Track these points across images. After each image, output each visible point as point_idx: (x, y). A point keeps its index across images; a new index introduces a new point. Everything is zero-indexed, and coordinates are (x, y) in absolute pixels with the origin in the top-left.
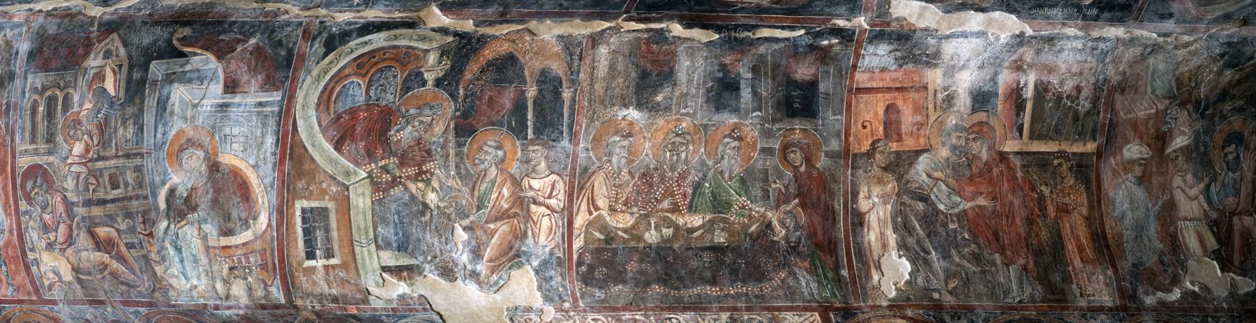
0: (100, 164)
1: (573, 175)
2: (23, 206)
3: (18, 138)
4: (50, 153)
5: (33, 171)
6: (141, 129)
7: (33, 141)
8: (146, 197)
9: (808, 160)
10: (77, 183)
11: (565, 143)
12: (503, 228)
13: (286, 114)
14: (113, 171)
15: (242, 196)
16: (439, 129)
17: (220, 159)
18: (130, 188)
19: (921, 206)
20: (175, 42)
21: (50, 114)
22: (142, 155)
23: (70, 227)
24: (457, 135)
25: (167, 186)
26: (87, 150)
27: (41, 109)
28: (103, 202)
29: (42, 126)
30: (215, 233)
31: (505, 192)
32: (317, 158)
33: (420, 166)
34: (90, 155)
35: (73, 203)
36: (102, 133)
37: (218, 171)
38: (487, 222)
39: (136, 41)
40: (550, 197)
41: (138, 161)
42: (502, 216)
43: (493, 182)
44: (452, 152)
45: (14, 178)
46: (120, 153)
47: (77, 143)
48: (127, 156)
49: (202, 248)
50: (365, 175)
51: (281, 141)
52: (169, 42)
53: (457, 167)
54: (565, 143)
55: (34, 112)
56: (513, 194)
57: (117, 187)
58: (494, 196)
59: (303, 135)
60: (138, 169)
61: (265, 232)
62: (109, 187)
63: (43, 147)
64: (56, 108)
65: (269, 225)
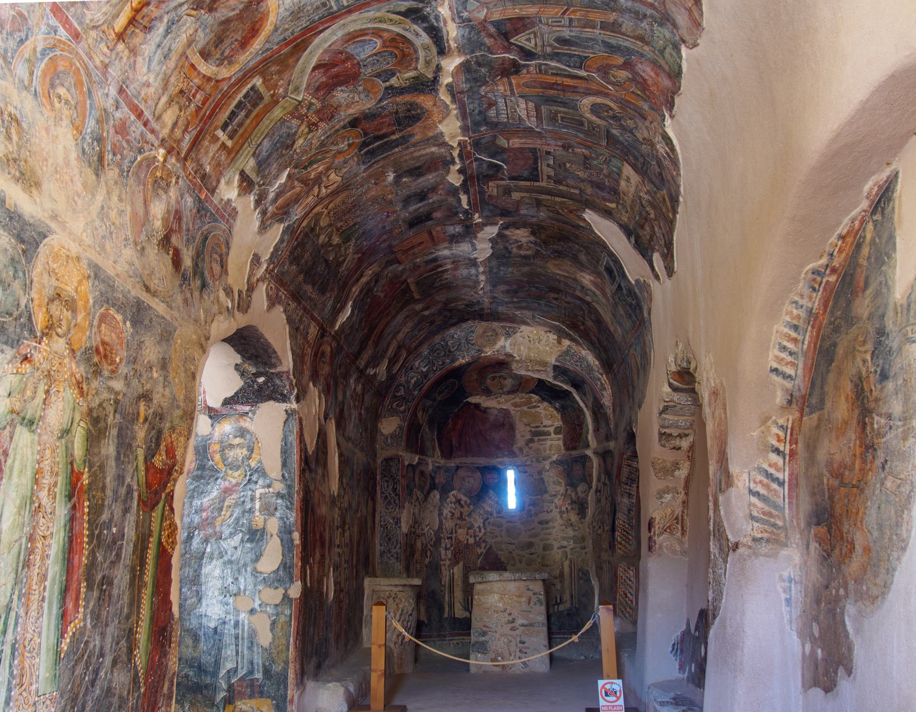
1: (344, 184)
9: (384, 240)
11: (363, 167)
12: (298, 187)
15: (244, 38)
16: (351, 111)
19: (373, 283)
24: (349, 123)
31: (320, 169)
32: (301, 62)
33: (321, 120)
38: (297, 179)
40: (326, 187)
42: (304, 182)
43: (324, 158)
44: (337, 127)
49: (180, 50)
50: (300, 99)
53: (327, 137)
54: (363, 167)
56: (321, 173)
58: (315, 166)
59: (317, 41)
61: (224, 80)
65: (230, 78)
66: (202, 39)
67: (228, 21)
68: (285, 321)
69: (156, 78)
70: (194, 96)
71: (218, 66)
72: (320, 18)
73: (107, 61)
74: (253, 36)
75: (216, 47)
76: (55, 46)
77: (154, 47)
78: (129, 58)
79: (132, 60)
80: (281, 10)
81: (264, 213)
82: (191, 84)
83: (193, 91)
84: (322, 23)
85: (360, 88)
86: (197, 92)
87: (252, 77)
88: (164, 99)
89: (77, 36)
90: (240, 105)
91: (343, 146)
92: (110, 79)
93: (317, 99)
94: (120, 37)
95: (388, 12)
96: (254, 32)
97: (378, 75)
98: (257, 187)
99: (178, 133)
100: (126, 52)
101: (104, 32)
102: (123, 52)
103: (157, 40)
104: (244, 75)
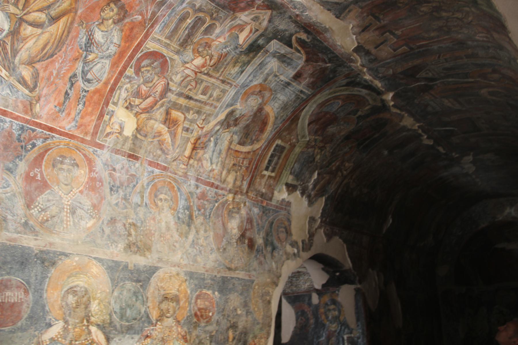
0: (204, 77)
2: (130, 72)
3: (157, 28)
4: (178, 52)
5: (154, 55)
6: (242, 72)
7: (170, 38)
8: (216, 107)
10: (183, 81)
12: (327, 177)
13: (306, 102)
14: (209, 84)
17: (265, 107)
18: (212, 99)
20: (294, 38)
21: (194, 27)
22: (231, 85)
23: (155, 103)
25: (232, 108)
26: (203, 66)
27: (189, 21)
28: (189, 98)
29: (182, 33)
30: (237, 141)
31: (337, 164)
34: (203, 70)
35: (170, 90)
36: (219, 60)
37: (260, 112)
39: (277, 23)
40: (346, 170)
41: (227, 87)
45: (136, 51)
46: (221, 78)
47: (200, 58)
48: (223, 82)
49: (226, 148)
51: (294, 112)
52: (291, 35)
55: (183, 19)
57: (205, 95)
58: (333, 164)
59: (303, 113)
60: (224, 92)
61: (257, 149)
62: (200, 92)
63: (175, 45)
64: (199, 28)
65: (261, 147)
66: (236, 138)
67: (247, 126)
68: (342, 243)
69: (217, 165)
70: (242, 163)
71: (251, 145)
72: (299, 105)
73: (186, 171)
74: (265, 126)
75: (247, 138)
76: (154, 179)
77: (211, 153)
78: (198, 164)
79: (200, 164)
80: (275, 109)
81: (309, 196)
82: (238, 159)
83: (241, 162)
84: (302, 106)
85: (342, 123)
86: (243, 161)
87: (274, 141)
88: (224, 173)
89: (165, 169)
90: (272, 156)
91: (347, 149)
92: (190, 177)
93: (319, 136)
94: (190, 158)
95: (337, 87)
96: (264, 123)
97: (349, 114)
98: (299, 187)
99: (238, 183)
100: (196, 162)
101: (180, 160)
102: (193, 163)
103: (212, 149)
104: (269, 143)
